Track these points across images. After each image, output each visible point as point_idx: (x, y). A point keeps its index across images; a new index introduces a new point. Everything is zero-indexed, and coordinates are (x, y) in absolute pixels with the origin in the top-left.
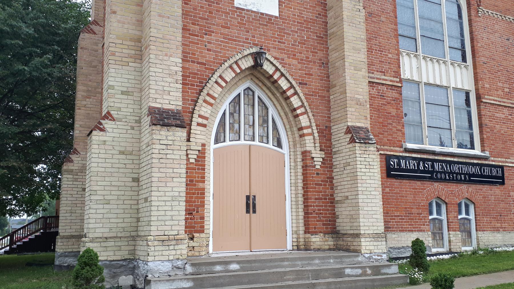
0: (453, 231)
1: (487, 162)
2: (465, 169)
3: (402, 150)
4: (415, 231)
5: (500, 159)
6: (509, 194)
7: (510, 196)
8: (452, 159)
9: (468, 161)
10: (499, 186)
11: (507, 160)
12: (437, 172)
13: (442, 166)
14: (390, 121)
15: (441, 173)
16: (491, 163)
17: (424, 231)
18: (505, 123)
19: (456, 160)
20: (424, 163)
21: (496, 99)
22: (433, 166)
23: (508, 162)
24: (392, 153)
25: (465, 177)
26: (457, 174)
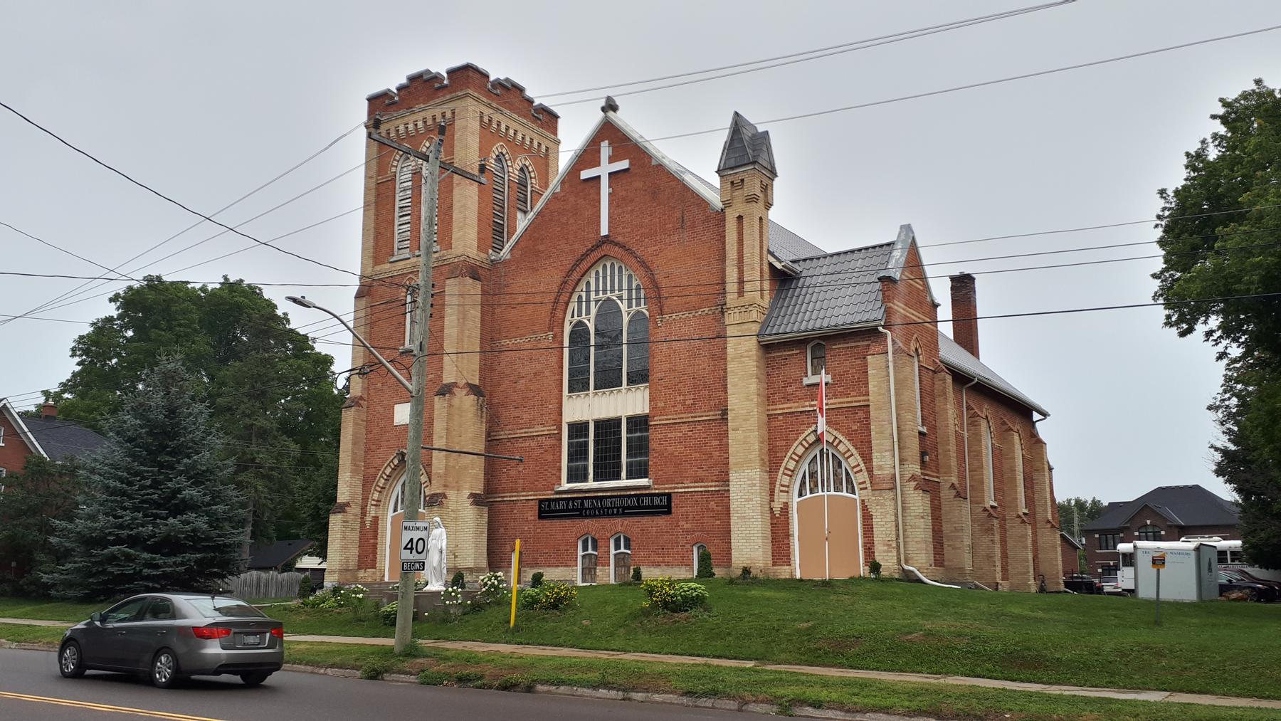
0: (602, 566)
1: (647, 492)
2: (618, 502)
3: (553, 492)
4: (562, 566)
5: (667, 486)
6: (677, 523)
7: (679, 526)
8: (604, 494)
9: (622, 493)
10: (663, 516)
11: (676, 485)
12: (586, 509)
13: (592, 503)
14: (546, 468)
15: (590, 509)
16: (653, 492)
17: (570, 566)
18: (682, 442)
19: (608, 494)
20: (573, 503)
21: (669, 417)
22: (582, 504)
23: (678, 488)
24: (544, 497)
25: (618, 511)
26: (608, 508)
